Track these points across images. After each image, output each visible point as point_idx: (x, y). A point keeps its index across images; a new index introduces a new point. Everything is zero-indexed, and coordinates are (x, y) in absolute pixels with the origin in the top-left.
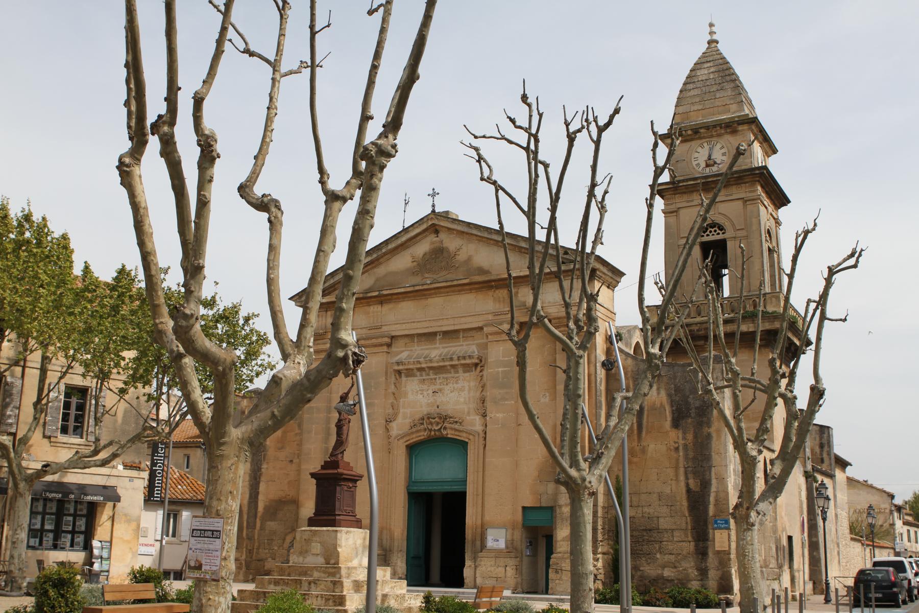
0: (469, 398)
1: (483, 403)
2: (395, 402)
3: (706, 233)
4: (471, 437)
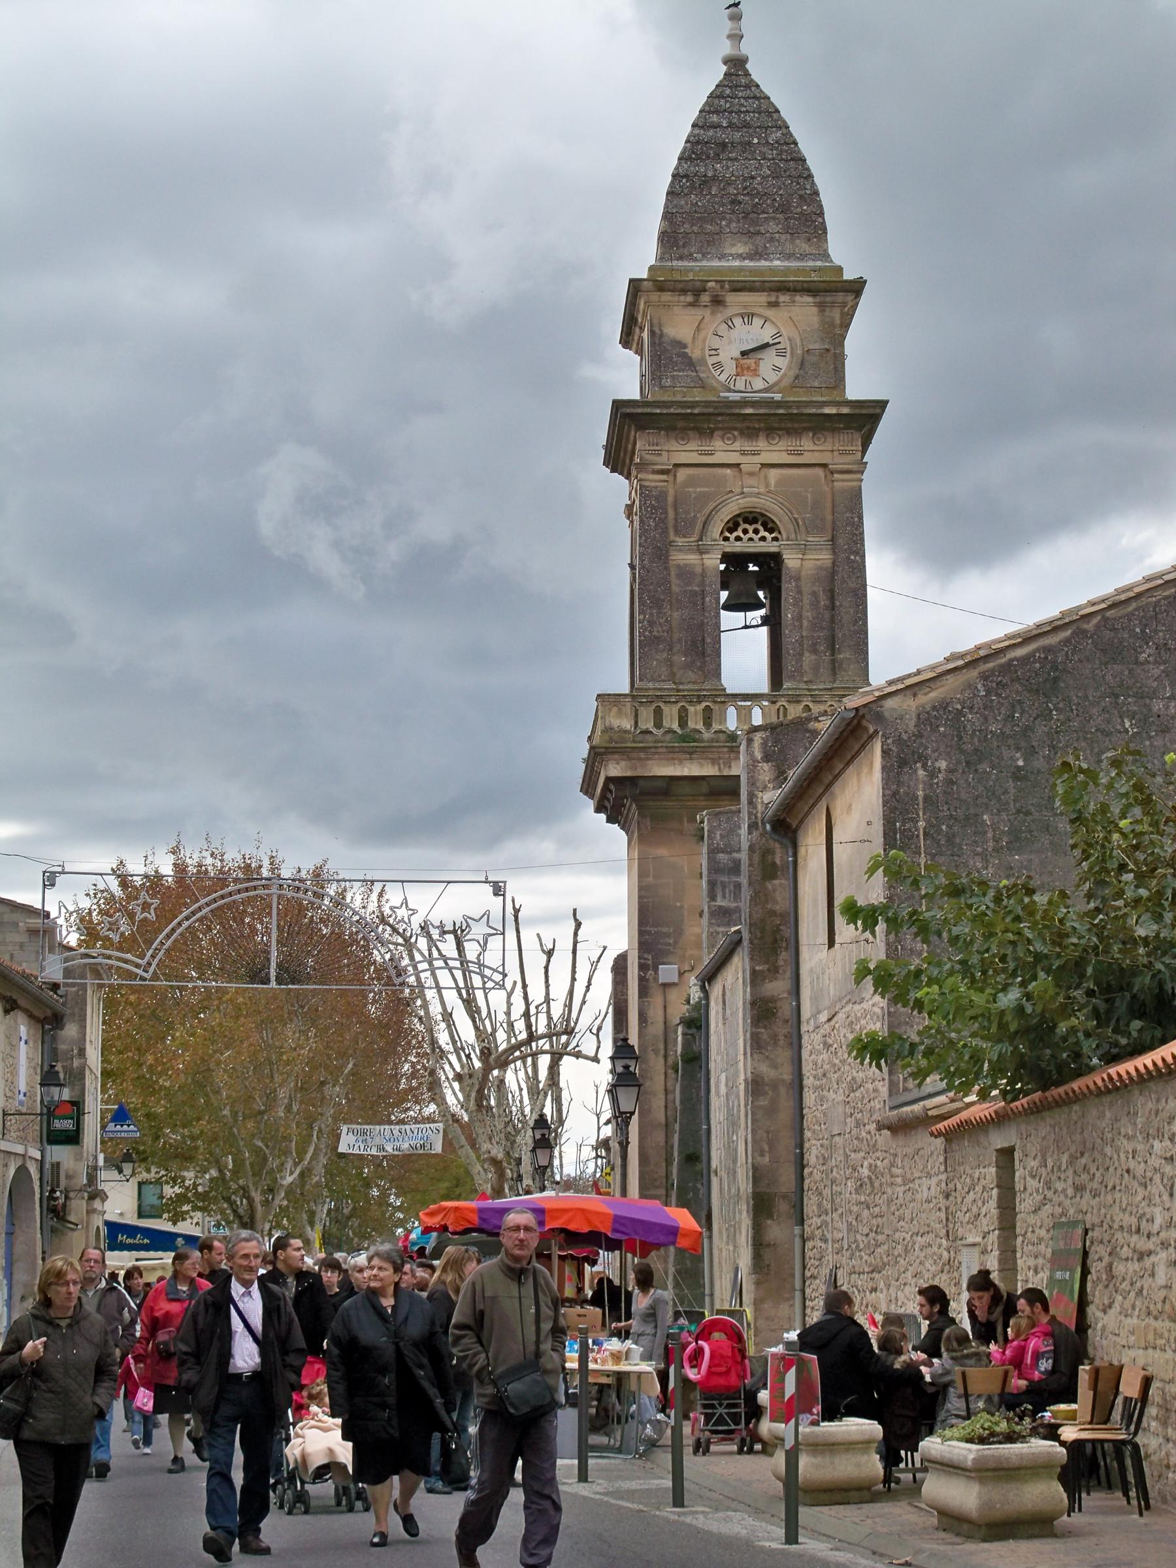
3: (735, 534)
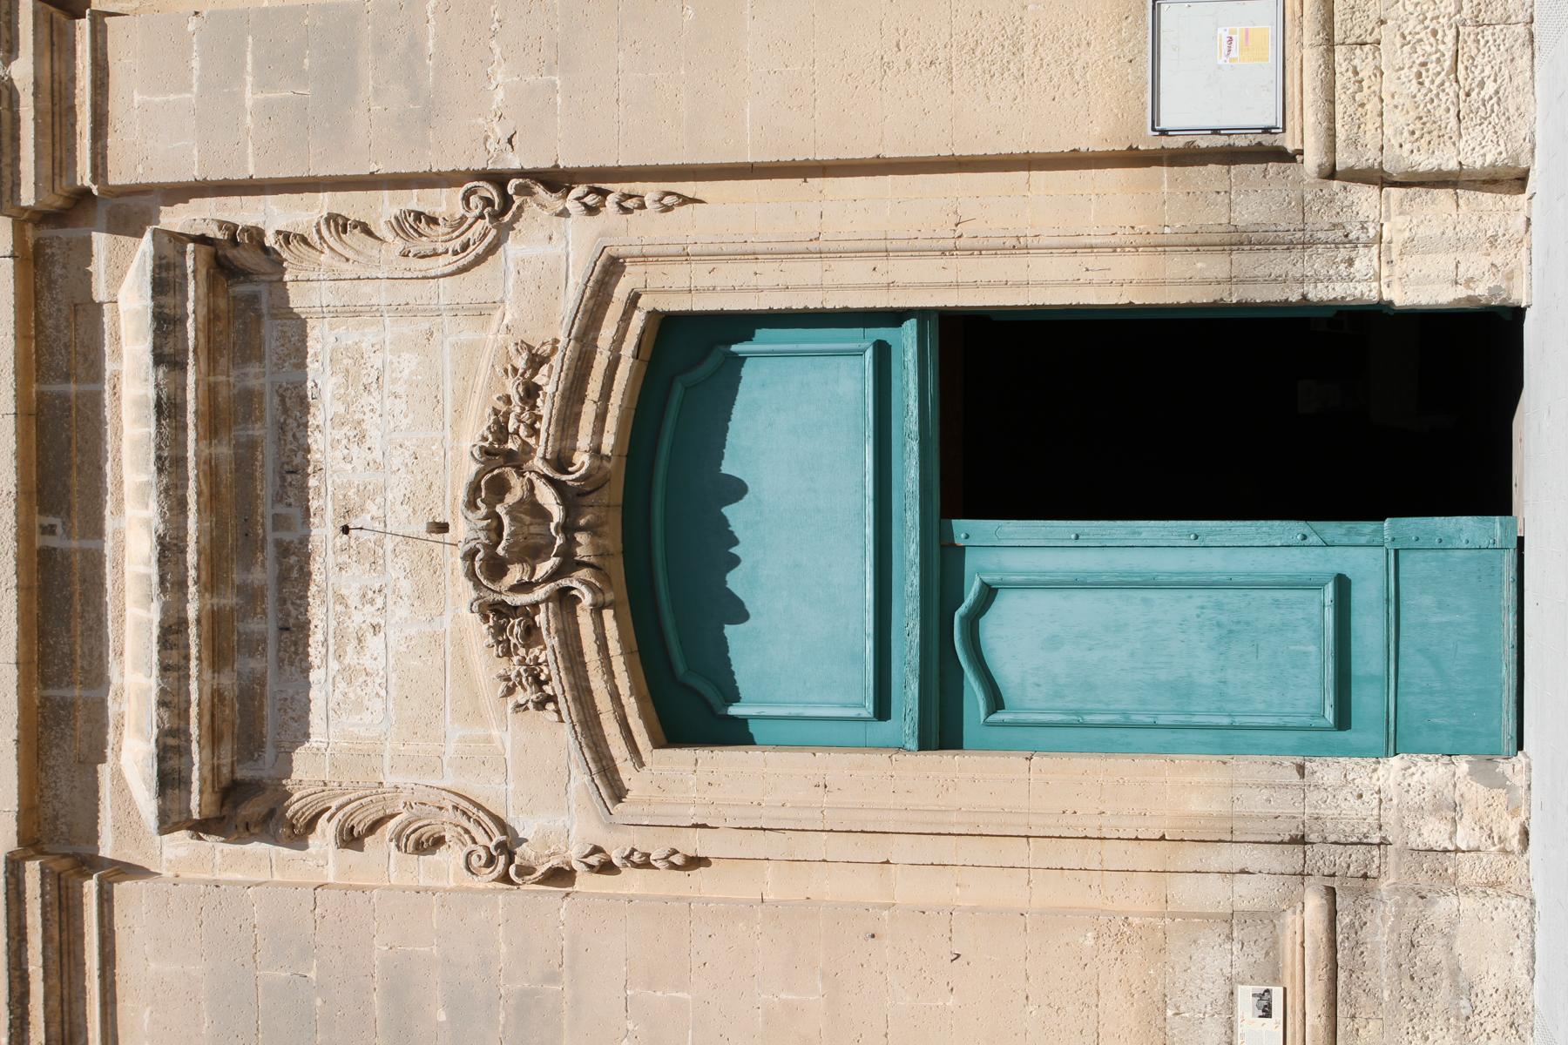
0: (403, 310)
1: (432, 221)
2: (391, 825)
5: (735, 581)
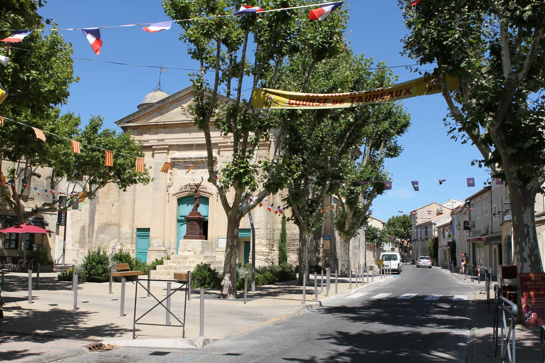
4: (210, 196)
5: (190, 205)
